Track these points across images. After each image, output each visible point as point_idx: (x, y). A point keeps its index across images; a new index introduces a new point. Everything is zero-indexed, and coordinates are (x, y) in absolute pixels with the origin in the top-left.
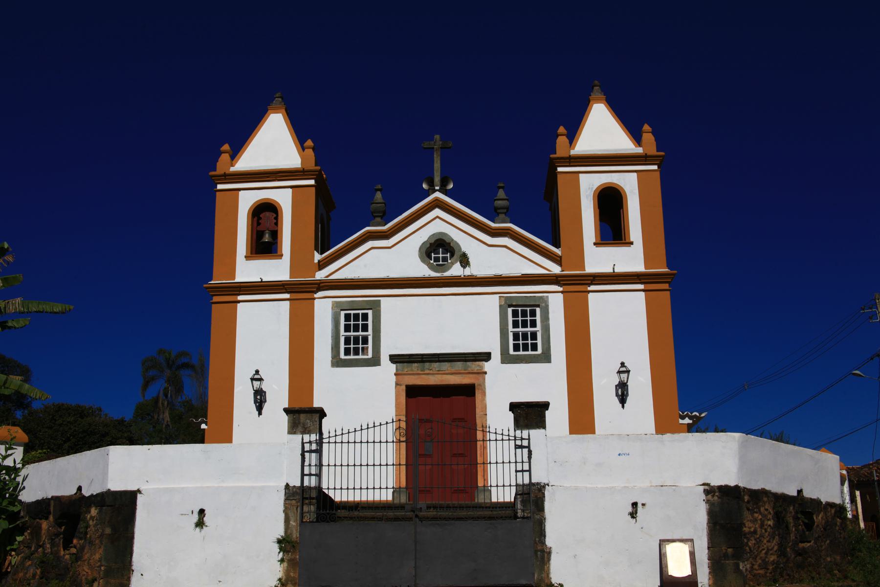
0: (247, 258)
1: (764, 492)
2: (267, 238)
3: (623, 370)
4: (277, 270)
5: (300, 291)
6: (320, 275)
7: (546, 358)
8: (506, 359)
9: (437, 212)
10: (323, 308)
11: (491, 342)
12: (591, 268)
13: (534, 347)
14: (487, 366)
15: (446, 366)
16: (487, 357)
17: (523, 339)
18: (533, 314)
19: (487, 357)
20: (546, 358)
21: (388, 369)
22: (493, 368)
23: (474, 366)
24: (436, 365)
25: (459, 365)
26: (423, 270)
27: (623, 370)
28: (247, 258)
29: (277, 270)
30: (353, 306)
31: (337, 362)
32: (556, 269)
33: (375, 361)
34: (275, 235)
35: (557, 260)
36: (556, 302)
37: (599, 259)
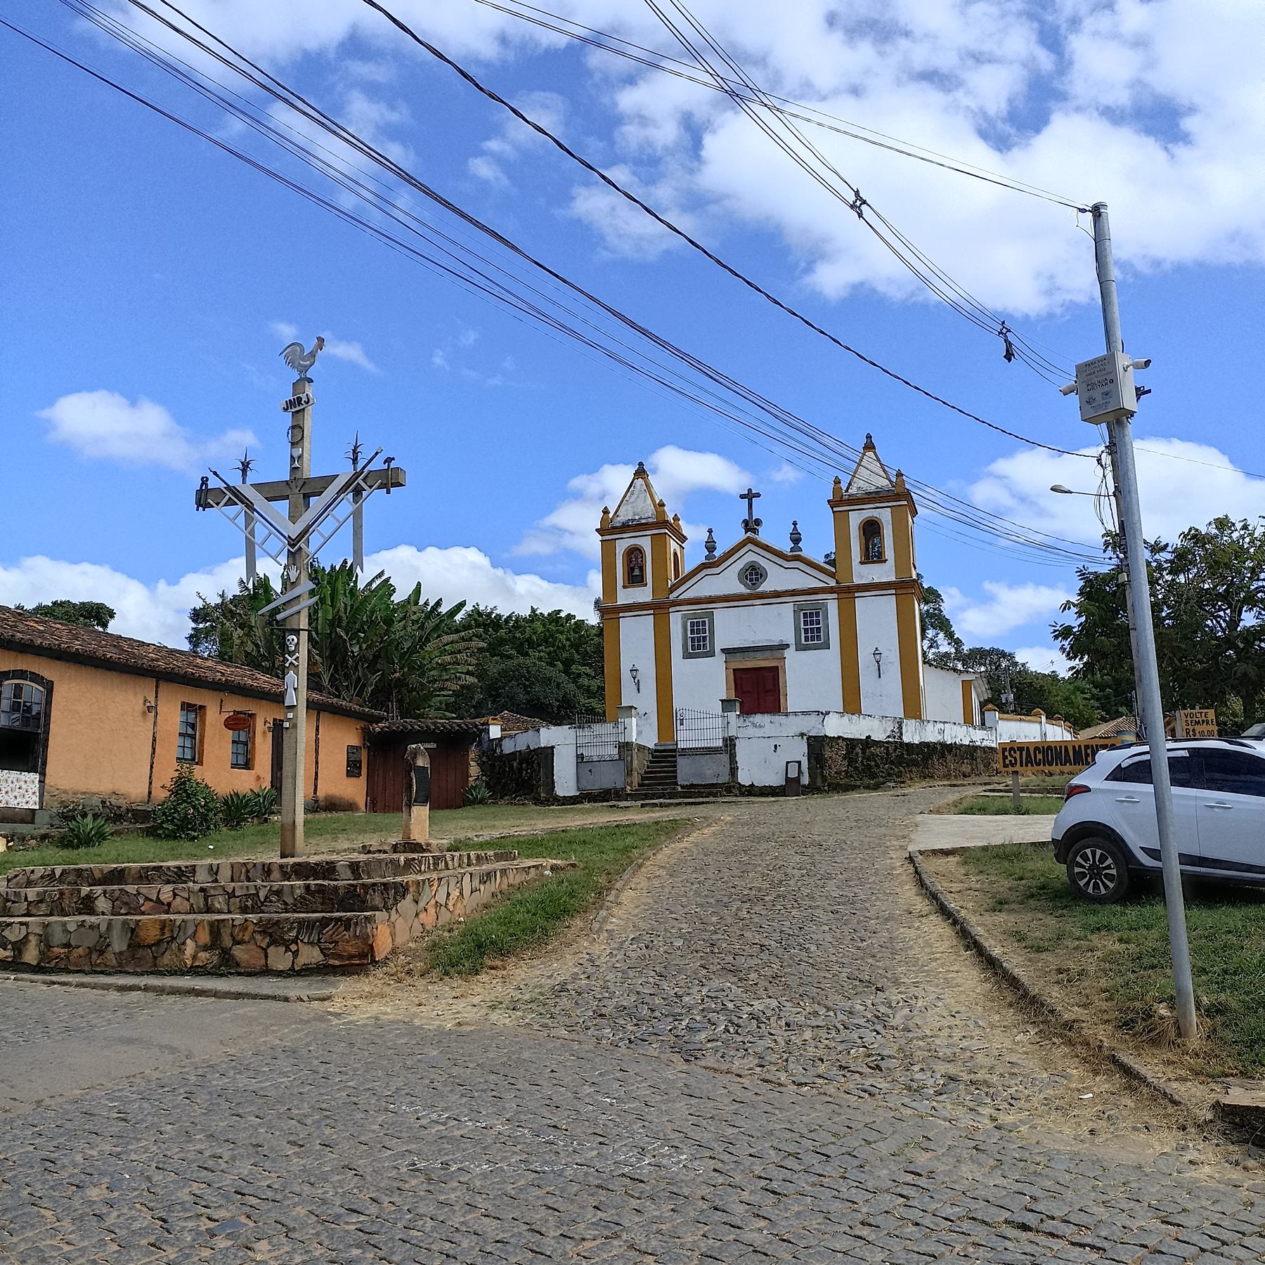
0: (624, 587)
1: (839, 737)
2: (637, 572)
3: (876, 653)
4: (643, 595)
5: (659, 609)
6: (673, 596)
7: (827, 646)
8: (800, 648)
9: (750, 546)
10: (676, 621)
11: (790, 638)
12: (857, 581)
13: (819, 638)
14: (787, 653)
15: (758, 655)
16: (788, 646)
17: (811, 634)
18: (817, 614)
19: (788, 646)
20: (827, 646)
21: (720, 659)
22: (790, 654)
23: (777, 654)
24: (752, 654)
25: (768, 654)
26: (742, 589)
27: (876, 653)
28: (624, 587)
29: (643, 595)
30: (695, 616)
31: (687, 656)
32: (833, 583)
33: (711, 654)
34: (642, 569)
35: (832, 575)
36: (833, 607)
37: (864, 574)
